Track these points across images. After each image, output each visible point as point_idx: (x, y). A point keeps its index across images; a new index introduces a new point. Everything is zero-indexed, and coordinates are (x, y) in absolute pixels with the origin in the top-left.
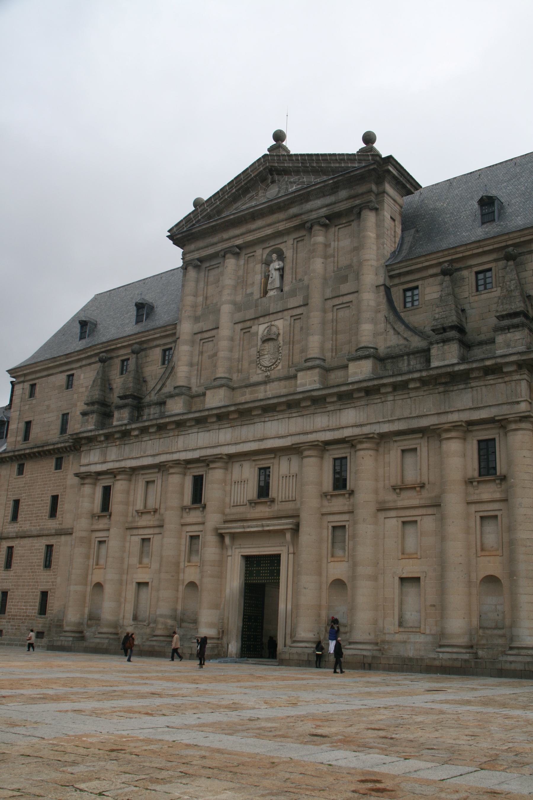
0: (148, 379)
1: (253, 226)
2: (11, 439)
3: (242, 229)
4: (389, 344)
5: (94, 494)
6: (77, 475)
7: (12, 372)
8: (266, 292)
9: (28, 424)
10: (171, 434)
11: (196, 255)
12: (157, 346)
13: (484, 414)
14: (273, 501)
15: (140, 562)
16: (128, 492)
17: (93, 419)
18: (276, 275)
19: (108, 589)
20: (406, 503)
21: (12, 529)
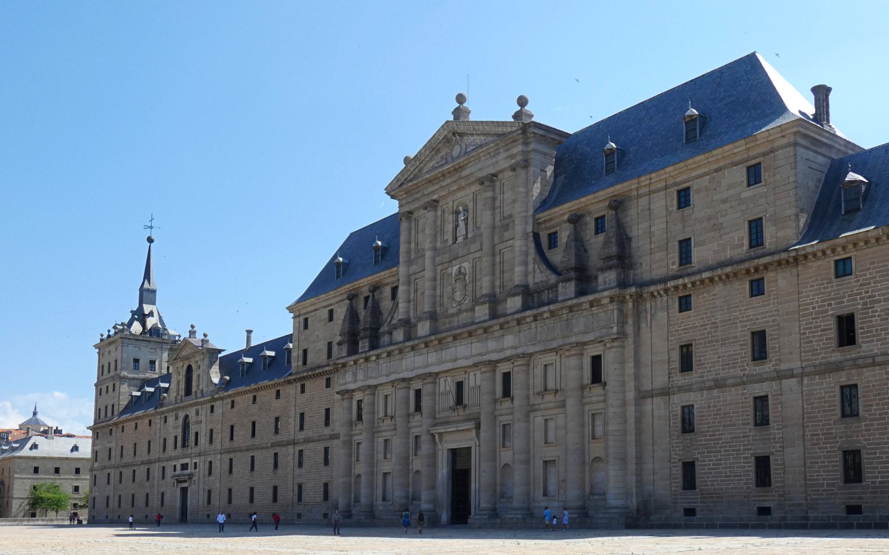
0: (383, 312)
1: (444, 184)
2: (294, 364)
3: (437, 187)
4: (537, 280)
5: (351, 406)
6: (338, 393)
7: (290, 309)
8: (456, 239)
9: (305, 352)
10: (397, 357)
11: (407, 209)
12: (387, 284)
13: (590, 337)
14: (465, 406)
15: (385, 458)
16: (374, 404)
17: (345, 348)
18: (462, 224)
19: (363, 479)
20: (547, 405)
21: (301, 436)
